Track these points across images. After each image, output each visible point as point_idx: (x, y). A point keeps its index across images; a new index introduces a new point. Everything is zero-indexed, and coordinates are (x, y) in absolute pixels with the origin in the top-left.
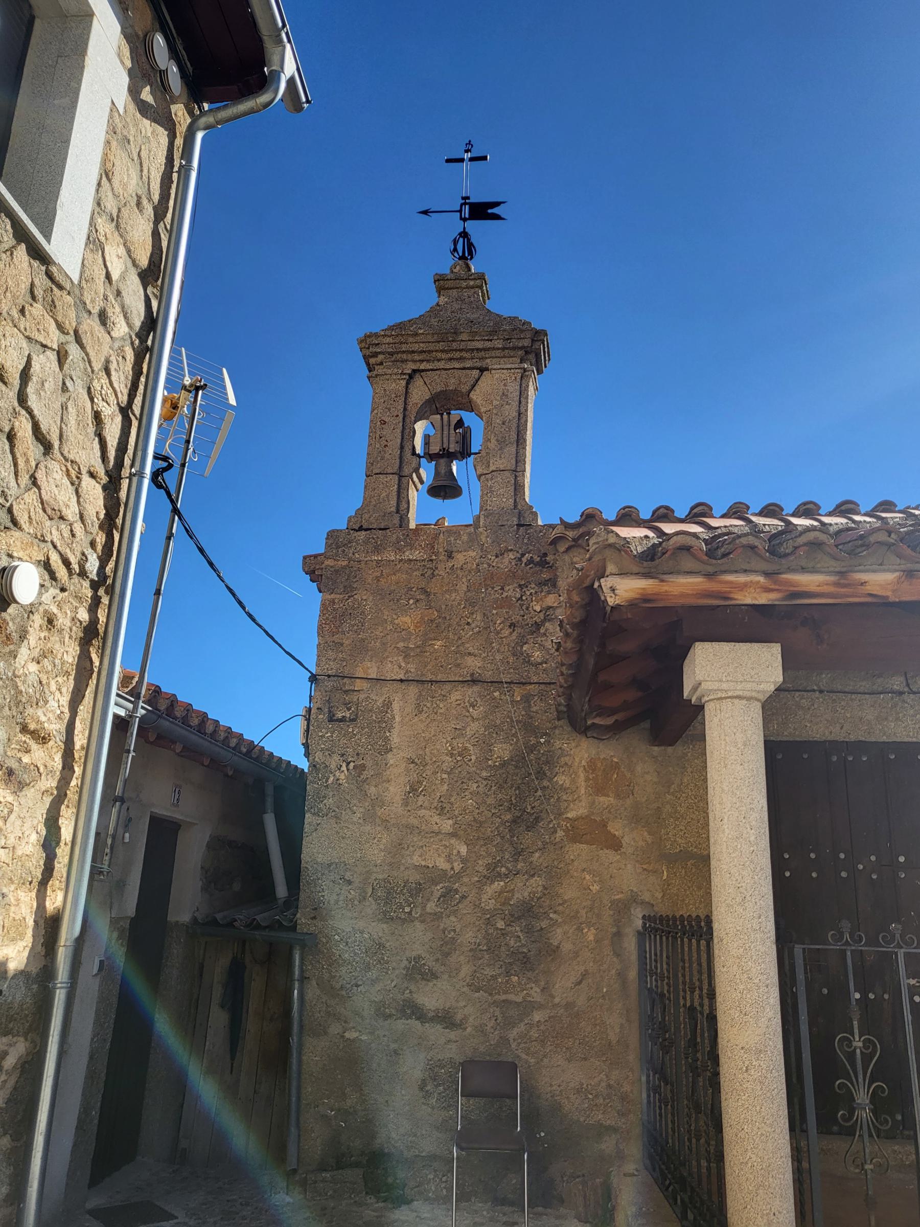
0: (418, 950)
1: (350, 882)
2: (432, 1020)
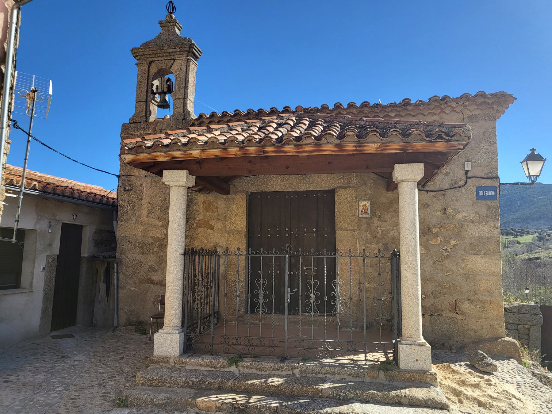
0: (152, 263)
1: (131, 242)
2: (156, 284)
